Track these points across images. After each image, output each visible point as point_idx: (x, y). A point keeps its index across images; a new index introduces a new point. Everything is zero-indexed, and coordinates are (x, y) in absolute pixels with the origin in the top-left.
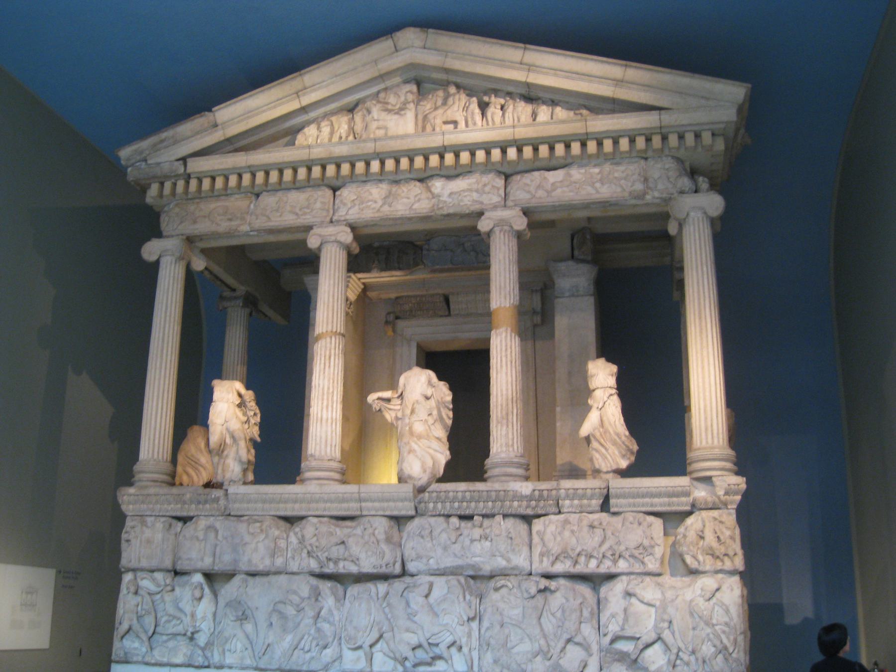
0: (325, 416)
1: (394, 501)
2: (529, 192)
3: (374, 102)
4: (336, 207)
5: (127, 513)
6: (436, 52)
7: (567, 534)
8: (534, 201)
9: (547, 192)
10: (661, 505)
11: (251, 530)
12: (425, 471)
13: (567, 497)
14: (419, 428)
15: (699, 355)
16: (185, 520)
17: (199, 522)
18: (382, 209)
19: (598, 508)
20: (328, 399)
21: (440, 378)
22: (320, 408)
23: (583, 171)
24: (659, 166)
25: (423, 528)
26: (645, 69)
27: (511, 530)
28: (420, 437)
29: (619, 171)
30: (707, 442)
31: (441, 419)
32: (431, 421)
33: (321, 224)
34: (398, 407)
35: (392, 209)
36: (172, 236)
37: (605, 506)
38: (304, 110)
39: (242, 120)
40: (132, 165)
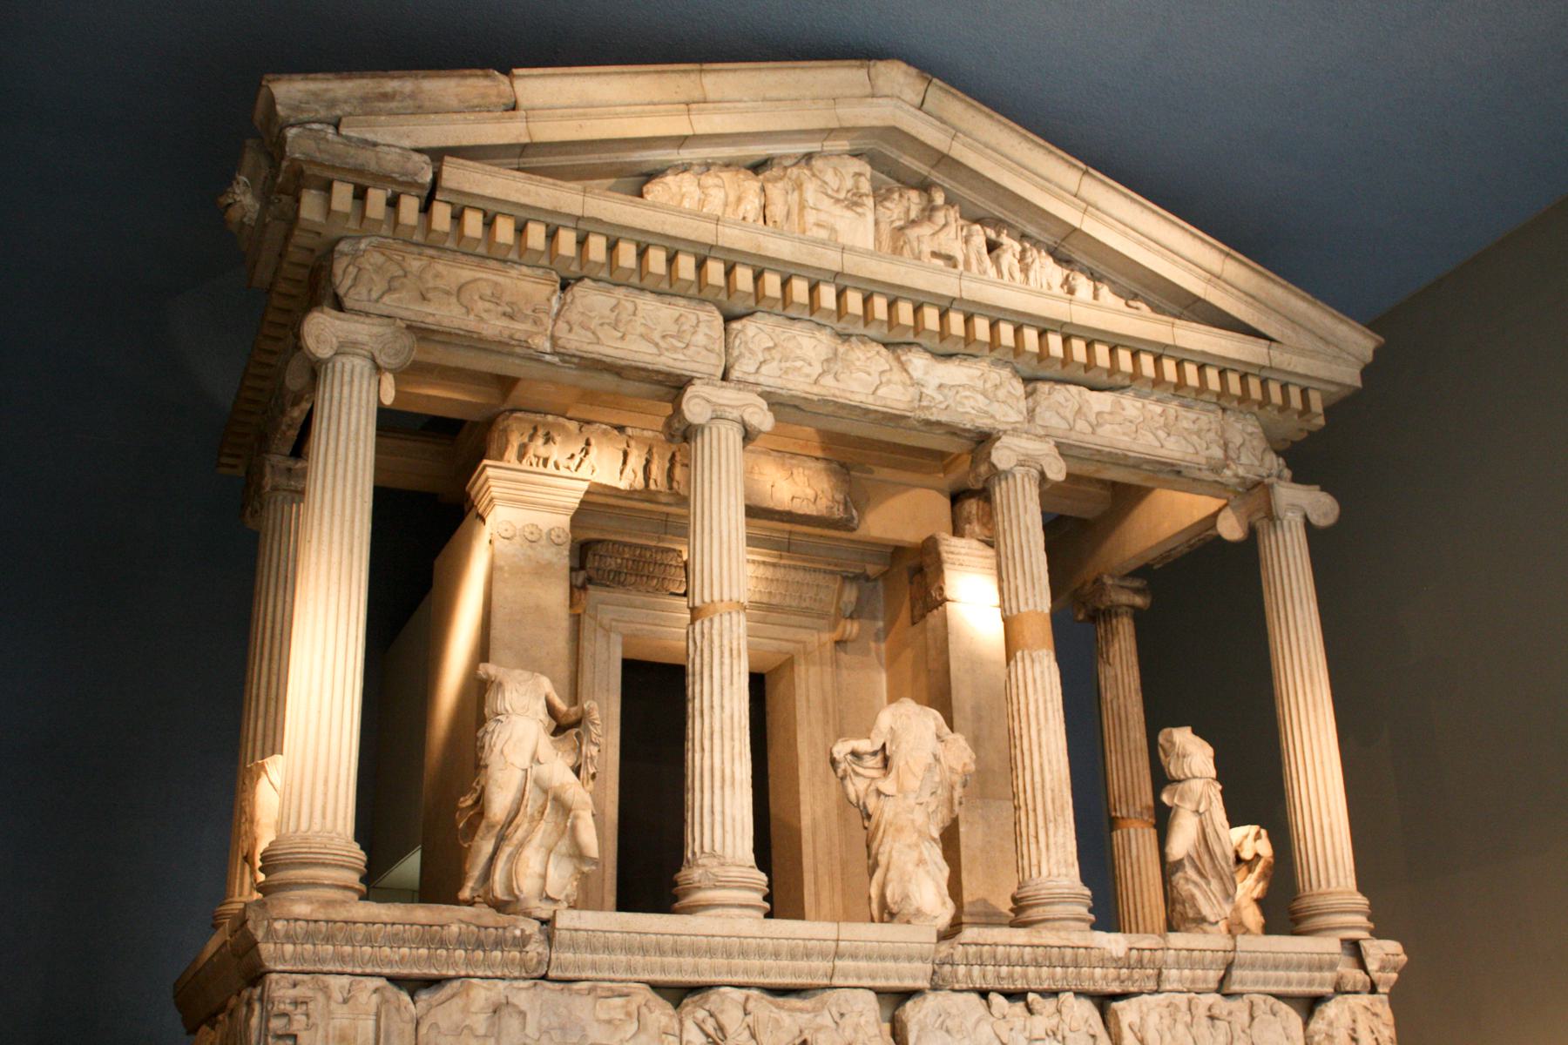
2: (1063, 418)
4: (736, 353)
5: (271, 965)
7: (1180, 1028)
8: (1074, 435)
10: (1300, 983)
11: (603, 1016)
16: (415, 985)
17: (473, 993)
18: (823, 381)
19: (1214, 985)
22: (727, 756)
23: (1139, 404)
24: (1239, 426)
26: (1253, 269)
29: (1187, 419)
34: (874, 773)
35: (841, 386)
36: (367, 314)
39: (571, 117)
40: (301, 124)
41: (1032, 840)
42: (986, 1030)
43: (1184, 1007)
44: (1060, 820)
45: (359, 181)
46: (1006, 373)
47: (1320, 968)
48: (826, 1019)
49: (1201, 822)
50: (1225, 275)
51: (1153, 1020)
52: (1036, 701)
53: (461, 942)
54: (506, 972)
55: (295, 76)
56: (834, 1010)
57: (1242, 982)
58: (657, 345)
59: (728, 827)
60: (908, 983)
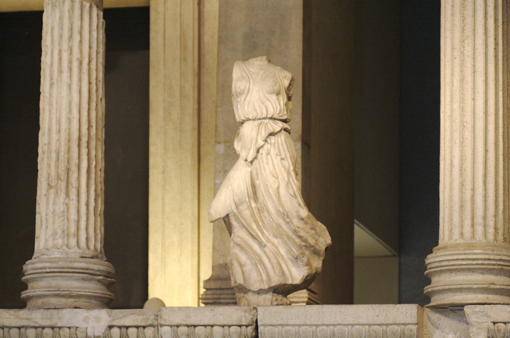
15: (457, 53)
30: (462, 234)
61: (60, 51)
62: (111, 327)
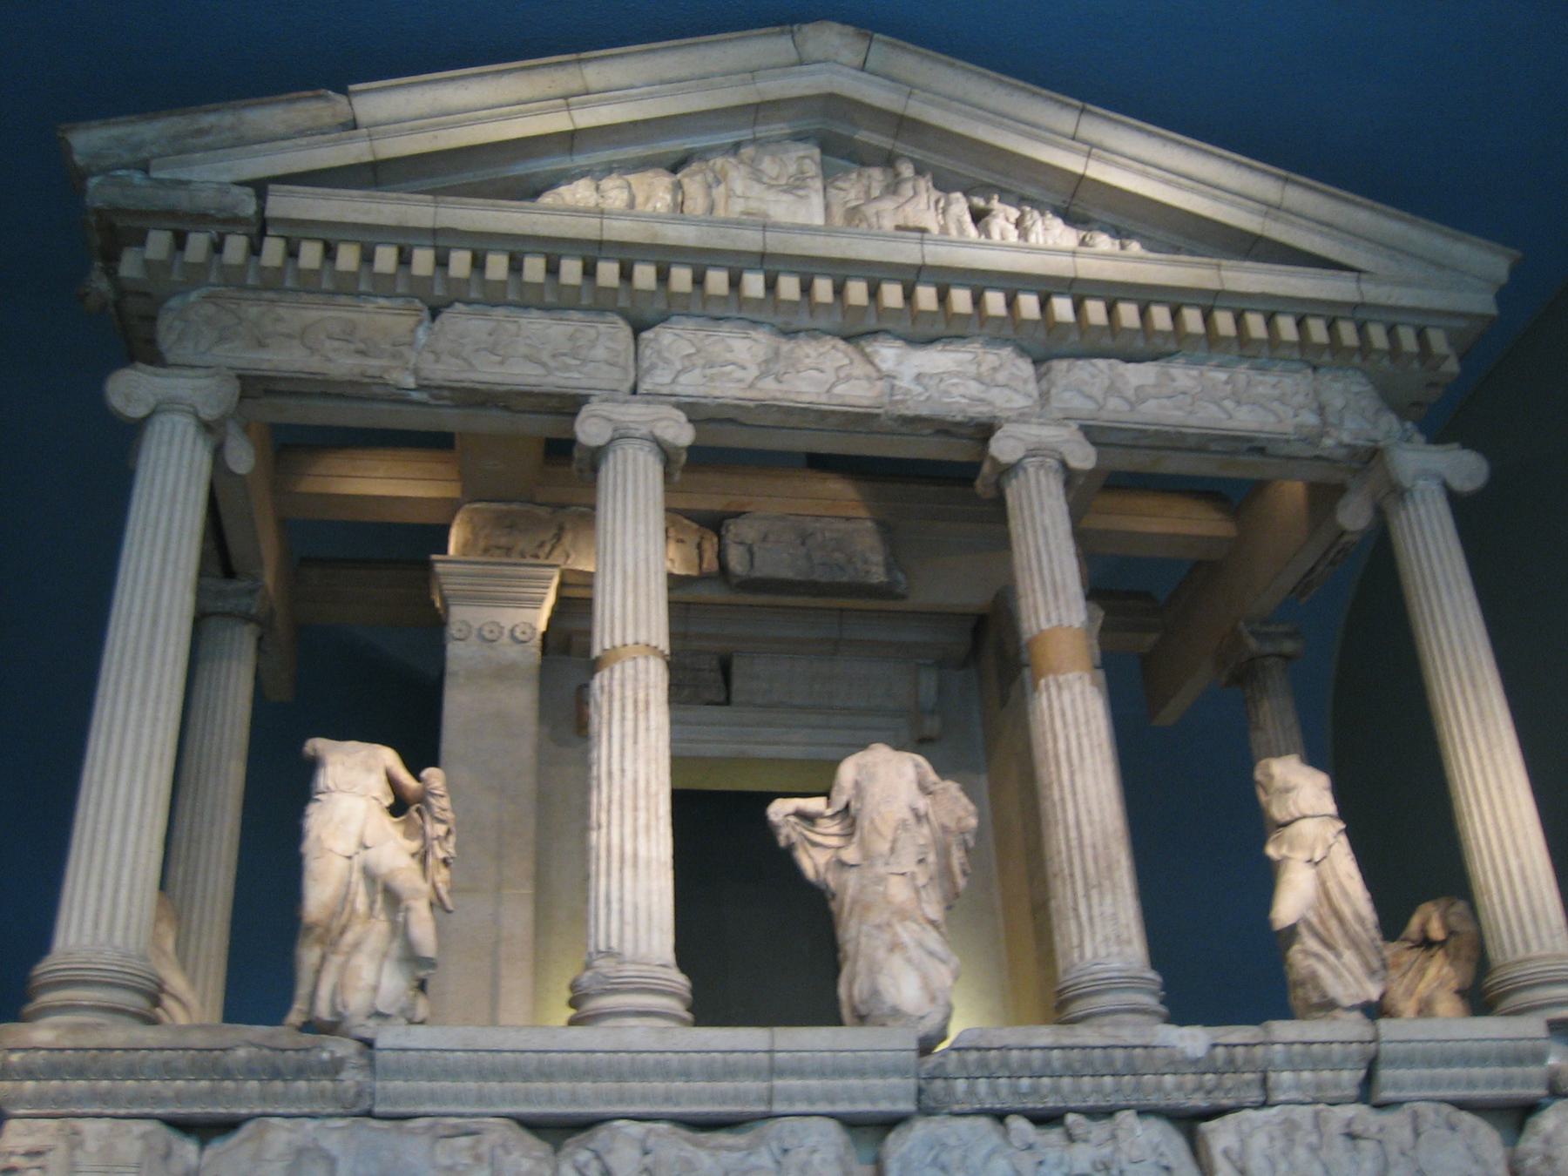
0: (642, 852)
1: (861, 1073)
2: (1090, 397)
3: (732, 160)
4: (645, 364)
6: (888, 83)
7: (1301, 1153)
8: (1104, 415)
9: (1126, 400)
10: (1491, 1083)
11: (444, 1160)
12: (933, 999)
13: (1293, 1065)
14: (899, 891)
18: (760, 384)
19: (1352, 1092)
20: (648, 810)
21: (943, 778)
22: (628, 830)
23: (1194, 373)
24: (1338, 386)
25: (944, 1146)
27: (1163, 1148)
28: (903, 915)
29: (1266, 384)
30: (1541, 945)
31: (946, 871)
32: (922, 880)
33: (611, 396)
34: (834, 841)
35: (784, 387)
36: (193, 367)
37: (1367, 1091)
38: (570, 140)
40: (104, 171)
41: (1071, 914)
42: (1000, 1165)
43: (1307, 1124)
44: (1107, 883)
45: (179, 226)
46: (1007, 352)
47: (1519, 1060)
48: (764, 1159)
49: (1319, 875)
50: (1286, 204)
51: (1259, 1142)
52: (1067, 738)
53: (249, 1071)
54: (316, 1108)
55: (93, 123)
56: (774, 1145)
57: (1397, 1085)
58: (544, 365)
59: (628, 916)
60: (884, 1106)
61: (1079, 737)
62: (1215, 1045)
